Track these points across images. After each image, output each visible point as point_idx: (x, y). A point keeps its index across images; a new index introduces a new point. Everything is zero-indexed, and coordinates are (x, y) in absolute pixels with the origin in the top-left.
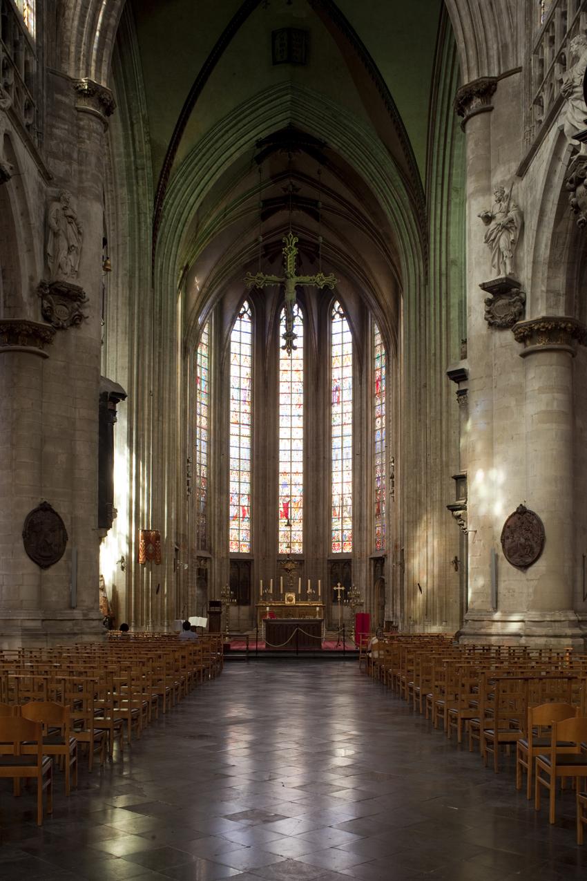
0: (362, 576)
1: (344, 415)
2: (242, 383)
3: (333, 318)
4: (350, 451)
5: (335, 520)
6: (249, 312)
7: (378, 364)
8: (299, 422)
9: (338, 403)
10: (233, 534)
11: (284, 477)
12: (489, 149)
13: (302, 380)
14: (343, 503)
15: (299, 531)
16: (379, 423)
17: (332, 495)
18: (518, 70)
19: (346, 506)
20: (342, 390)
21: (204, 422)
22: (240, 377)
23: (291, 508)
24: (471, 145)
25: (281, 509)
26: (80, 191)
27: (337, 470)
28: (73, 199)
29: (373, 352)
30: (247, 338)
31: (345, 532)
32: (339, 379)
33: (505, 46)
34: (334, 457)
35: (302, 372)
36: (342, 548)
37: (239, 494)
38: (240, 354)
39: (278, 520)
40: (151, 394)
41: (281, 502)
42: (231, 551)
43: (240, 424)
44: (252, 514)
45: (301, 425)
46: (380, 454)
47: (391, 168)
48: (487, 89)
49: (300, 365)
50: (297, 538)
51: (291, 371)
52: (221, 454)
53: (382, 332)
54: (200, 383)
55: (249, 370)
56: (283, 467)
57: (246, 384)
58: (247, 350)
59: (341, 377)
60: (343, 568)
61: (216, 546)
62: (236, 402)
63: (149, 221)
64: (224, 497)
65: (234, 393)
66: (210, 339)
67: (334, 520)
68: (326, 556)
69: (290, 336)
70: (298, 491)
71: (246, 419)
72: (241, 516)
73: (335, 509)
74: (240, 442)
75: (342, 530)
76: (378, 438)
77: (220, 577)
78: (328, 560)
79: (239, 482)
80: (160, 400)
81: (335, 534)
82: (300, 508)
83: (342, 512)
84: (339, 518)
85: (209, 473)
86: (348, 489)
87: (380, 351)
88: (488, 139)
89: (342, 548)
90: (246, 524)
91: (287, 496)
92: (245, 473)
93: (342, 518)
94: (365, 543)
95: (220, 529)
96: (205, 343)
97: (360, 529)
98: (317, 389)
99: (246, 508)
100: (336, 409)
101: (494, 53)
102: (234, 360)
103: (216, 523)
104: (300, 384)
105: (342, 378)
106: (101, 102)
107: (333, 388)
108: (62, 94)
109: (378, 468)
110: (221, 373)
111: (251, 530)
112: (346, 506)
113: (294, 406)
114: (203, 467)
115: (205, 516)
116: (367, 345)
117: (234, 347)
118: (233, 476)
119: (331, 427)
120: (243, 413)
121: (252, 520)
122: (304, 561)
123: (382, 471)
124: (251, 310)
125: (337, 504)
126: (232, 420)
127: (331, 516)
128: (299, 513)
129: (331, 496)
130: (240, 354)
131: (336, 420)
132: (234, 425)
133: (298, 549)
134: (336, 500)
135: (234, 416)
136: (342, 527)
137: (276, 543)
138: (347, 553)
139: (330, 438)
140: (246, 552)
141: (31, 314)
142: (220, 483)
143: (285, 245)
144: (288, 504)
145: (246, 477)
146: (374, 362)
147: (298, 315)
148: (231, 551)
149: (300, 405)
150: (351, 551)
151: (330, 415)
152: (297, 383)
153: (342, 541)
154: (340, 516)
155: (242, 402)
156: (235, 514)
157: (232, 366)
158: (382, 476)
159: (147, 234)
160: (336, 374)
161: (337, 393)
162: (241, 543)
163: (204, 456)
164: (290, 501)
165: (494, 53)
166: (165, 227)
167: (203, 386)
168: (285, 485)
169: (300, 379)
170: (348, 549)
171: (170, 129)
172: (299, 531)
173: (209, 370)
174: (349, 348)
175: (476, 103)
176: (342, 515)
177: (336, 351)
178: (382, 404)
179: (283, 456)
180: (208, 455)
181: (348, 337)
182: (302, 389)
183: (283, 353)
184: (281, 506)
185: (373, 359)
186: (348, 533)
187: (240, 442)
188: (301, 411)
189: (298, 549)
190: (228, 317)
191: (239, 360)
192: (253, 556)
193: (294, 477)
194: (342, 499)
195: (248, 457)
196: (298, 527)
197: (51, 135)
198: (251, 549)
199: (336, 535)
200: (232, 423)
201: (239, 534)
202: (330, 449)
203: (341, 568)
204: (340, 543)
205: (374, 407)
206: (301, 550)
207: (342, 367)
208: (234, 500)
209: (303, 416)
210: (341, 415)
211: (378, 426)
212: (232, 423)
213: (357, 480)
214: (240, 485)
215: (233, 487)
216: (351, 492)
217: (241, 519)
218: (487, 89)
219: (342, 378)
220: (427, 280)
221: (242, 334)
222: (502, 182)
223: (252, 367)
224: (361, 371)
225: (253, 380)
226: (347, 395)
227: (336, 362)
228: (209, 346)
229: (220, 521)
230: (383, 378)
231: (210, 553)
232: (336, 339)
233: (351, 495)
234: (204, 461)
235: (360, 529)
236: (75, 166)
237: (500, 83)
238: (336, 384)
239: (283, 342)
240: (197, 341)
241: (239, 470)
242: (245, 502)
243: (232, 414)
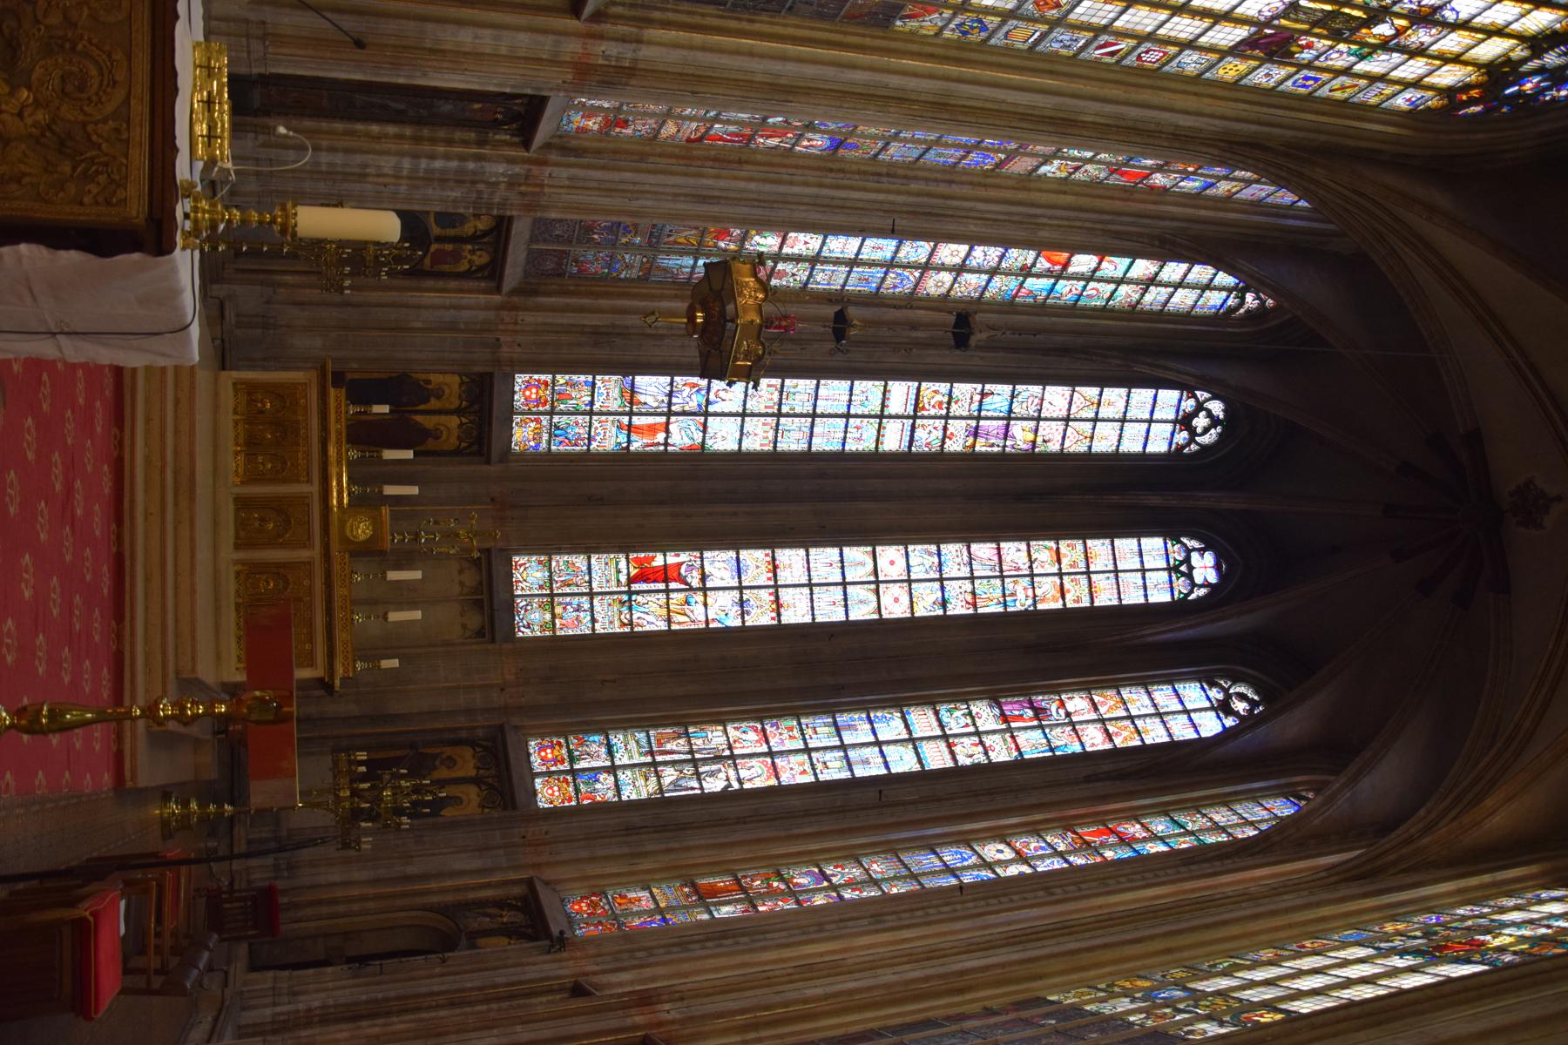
1: (976, 739)
2: (1025, 423)
3: (1212, 684)
4: (877, 770)
5: (644, 742)
6: (1194, 447)
9: (1004, 718)
10: (576, 387)
11: (764, 568)
13: (1040, 607)
14: (705, 761)
15: (594, 620)
17: (723, 723)
19: (698, 775)
20: (1041, 727)
22: (1038, 419)
23: (667, 591)
27: (809, 732)
31: (606, 781)
32: (1068, 714)
34: (842, 719)
35: (1059, 605)
36: (549, 774)
37: (707, 414)
38: (1095, 420)
39: (625, 549)
41: (684, 557)
42: (520, 379)
43: (915, 417)
44: (642, 457)
45: (920, 612)
46: (904, 872)
49: (1077, 601)
50: (570, 615)
51: (1060, 575)
54: (1048, 274)
55: (1054, 447)
56: (791, 560)
59: (1075, 719)
60: (476, 781)
61: (541, 318)
62: (975, 406)
67: (641, 736)
68: (516, 721)
70: (722, 611)
71: (928, 437)
72: (635, 419)
73: (679, 737)
74: (863, 416)
75: (612, 769)
78: (501, 728)
79: (743, 415)
81: (595, 743)
82: (669, 621)
83: (673, 763)
84: (651, 753)
86: (756, 776)
89: (549, 774)
90: (608, 438)
91: (704, 578)
92: (771, 435)
93: (654, 764)
94: (584, 854)
96: (1148, 298)
97: (630, 830)
99: (661, 437)
103: (619, 320)
104: (1030, 601)
105: (1072, 724)
109: (856, 872)
111: (588, 456)
112: (698, 775)
113: (967, 586)
114: (802, 272)
116: (1225, 783)
119: (931, 702)
120: (945, 429)
121: (623, 457)
122: (493, 641)
123: (851, 884)
124: (1196, 453)
125: (698, 743)
126: (928, 387)
127: (656, 726)
128: (651, 618)
129: (721, 721)
130: (1095, 420)
132: (913, 396)
133: (531, 621)
135: (939, 398)
136: (625, 767)
137: (548, 545)
138: (535, 793)
139: (899, 704)
140: (514, 439)
144: (683, 581)
145: (758, 439)
146: (1159, 814)
147: (1193, 585)
148: (520, 379)
149: (975, 605)
150: (543, 804)
151: (966, 699)
152: (1030, 592)
153: (573, 772)
154: (659, 758)
155: (973, 423)
156: (642, 398)
157: (1066, 390)
158: (834, 887)
161: (1030, 713)
162: (545, 420)
164: (691, 589)
169: (1043, 600)
170: (548, 794)
172: (594, 620)
176: (665, 763)
178: (1061, 855)
182: (1019, 608)
184: (672, 559)
185: (1164, 811)
186: (604, 789)
187: (863, 416)
188: (958, 608)
189: (531, 621)
191: (1084, 415)
192: (501, 461)
193: (765, 595)
194: (718, 758)
195: (820, 444)
198: (524, 457)
200: (918, 389)
201: (577, 413)
202: (865, 707)
204: (566, 766)
206: (528, 633)
207: (1102, 721)
209: (945, 617)
210: (972, 729)
212: (918, 389)
213: (795, 802)
216: (747, 786)
217: (625, 420)
219: (1072, 724)
224: (1122, 776)
225: (1032, 460)
226: (1032, 744)
230: (1137, 847)
231: (515, 292)
233: (736, 786)
235: (630, 830)
238: (1054, 707)
241: (779, 415)
242: (682, 435)
243: (943, 387)
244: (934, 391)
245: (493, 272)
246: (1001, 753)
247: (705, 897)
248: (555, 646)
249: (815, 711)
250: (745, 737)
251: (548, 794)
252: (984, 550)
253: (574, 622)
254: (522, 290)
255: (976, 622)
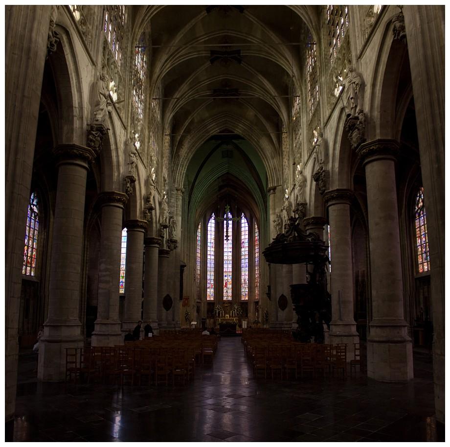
0: (251, 308)
7: (256, 235)
8: (230, 254)
12: (275, 203)
16: (257, 255)
18: (281, 185)
21: (199, 255)
24: (271, 201)
25: (225, 285)
26: (177, 214)
28: (175, 217)
29: (255, 231)
30: (213, 225)
33: (278, 178)
40: (187, 255)
42: (208, 299)
44: (214, 286)
47: (256, 186)
48: (274, 189)
52: (204, 266)
53: (257, 224)
55: (214, 236)
57: (213, 241)
58: (213, 229)
63: (187, 203)
64: (205, 281)
65: (209, 244)
66: (201, 226)
69: (227, 236)
71: (213, 253)
76: (256, 260)
77: (204, 308)
80: (190, 256)
85: (200, 272)
86: (247, 277)
87: (257, 230)
88: (275, 200)
90: (212, 290)
95: (204, 292)
98: (236, 242)
100: (243, 249)
101: (275, 180)
102: (209, 233)
106: (182, 191)
107: (242, 242)
108: (173, 191)
110: (205, 238)
115: (199, 287)
117: (209, 228)
118: (208, 273)
121: (214, 289)
126: (208, 254)
131: (243, 253)
133: (230, 298)
134: (243, 281)
137: (223, 296)
141: (165, 248)
142: (204, 275)
143: (226, 208)
145: (213, 273)
148: (208, 299)
159: (186, 207)
160: (243, 237)
163: (199, 267)
165: (275, 180)
166: (191, 204)
167: (199, 243)
168: (226, 276)
170: (247, 299)
171: (194, 177)
173: (201, 237)
174: (247, 228)
175: (272, 191)
177: (243, 229)
179: (225, 266)
180: (200, 266)
181: (247, 224)
183: (225, 242)
188: (231, 250)
189: (230, 298)
190: (208, 218)
196: (230, 291)
197: (171, 202)
198: (214, 299)
199: (243, 294)
203: (244, 304)
205: (255, 249)
208: (208, 282)
211: (256, 256)
214: (211, 276)
215: (208, 277)
218: (274, 189)
220: (267, 220)
221: (212, 225)
222: (278, 212)
223: (215, 235)
226: (247, 245)
227: (243, 233)
228: (201, 229)
229: (204, 290)
232: (243, 225)
234: (199, 269)
236: (176, 208)
237: (277, 187)
239: (225, 238)
240: (198, 228)
243: (208, 252)
244: (209, 253)
245: (199, 302)
246: (247, 249)
247: (257, 286)
248: (232, 296)
249: (241, 269)
250: (243, 278)
251: (247, 299)
252: (225, 246)
253: (230, 294)
254: (201, 300)
255: (233, 248)
